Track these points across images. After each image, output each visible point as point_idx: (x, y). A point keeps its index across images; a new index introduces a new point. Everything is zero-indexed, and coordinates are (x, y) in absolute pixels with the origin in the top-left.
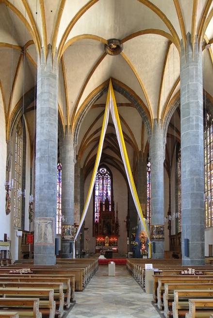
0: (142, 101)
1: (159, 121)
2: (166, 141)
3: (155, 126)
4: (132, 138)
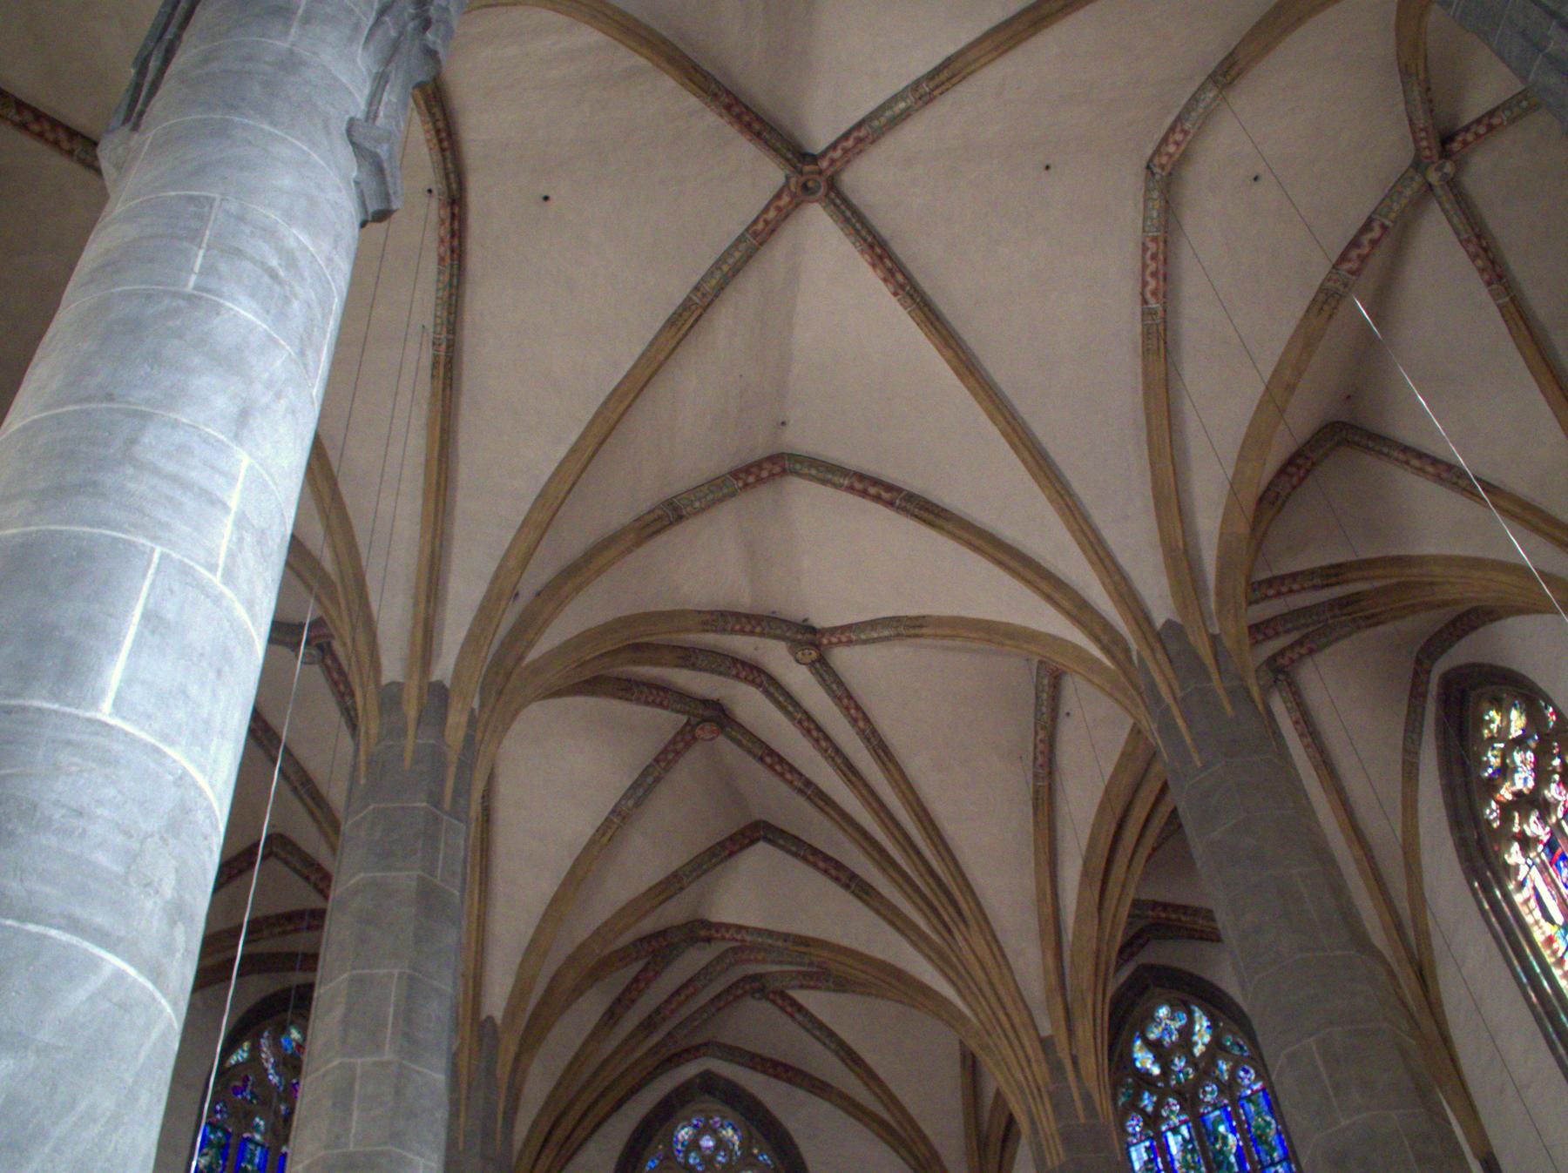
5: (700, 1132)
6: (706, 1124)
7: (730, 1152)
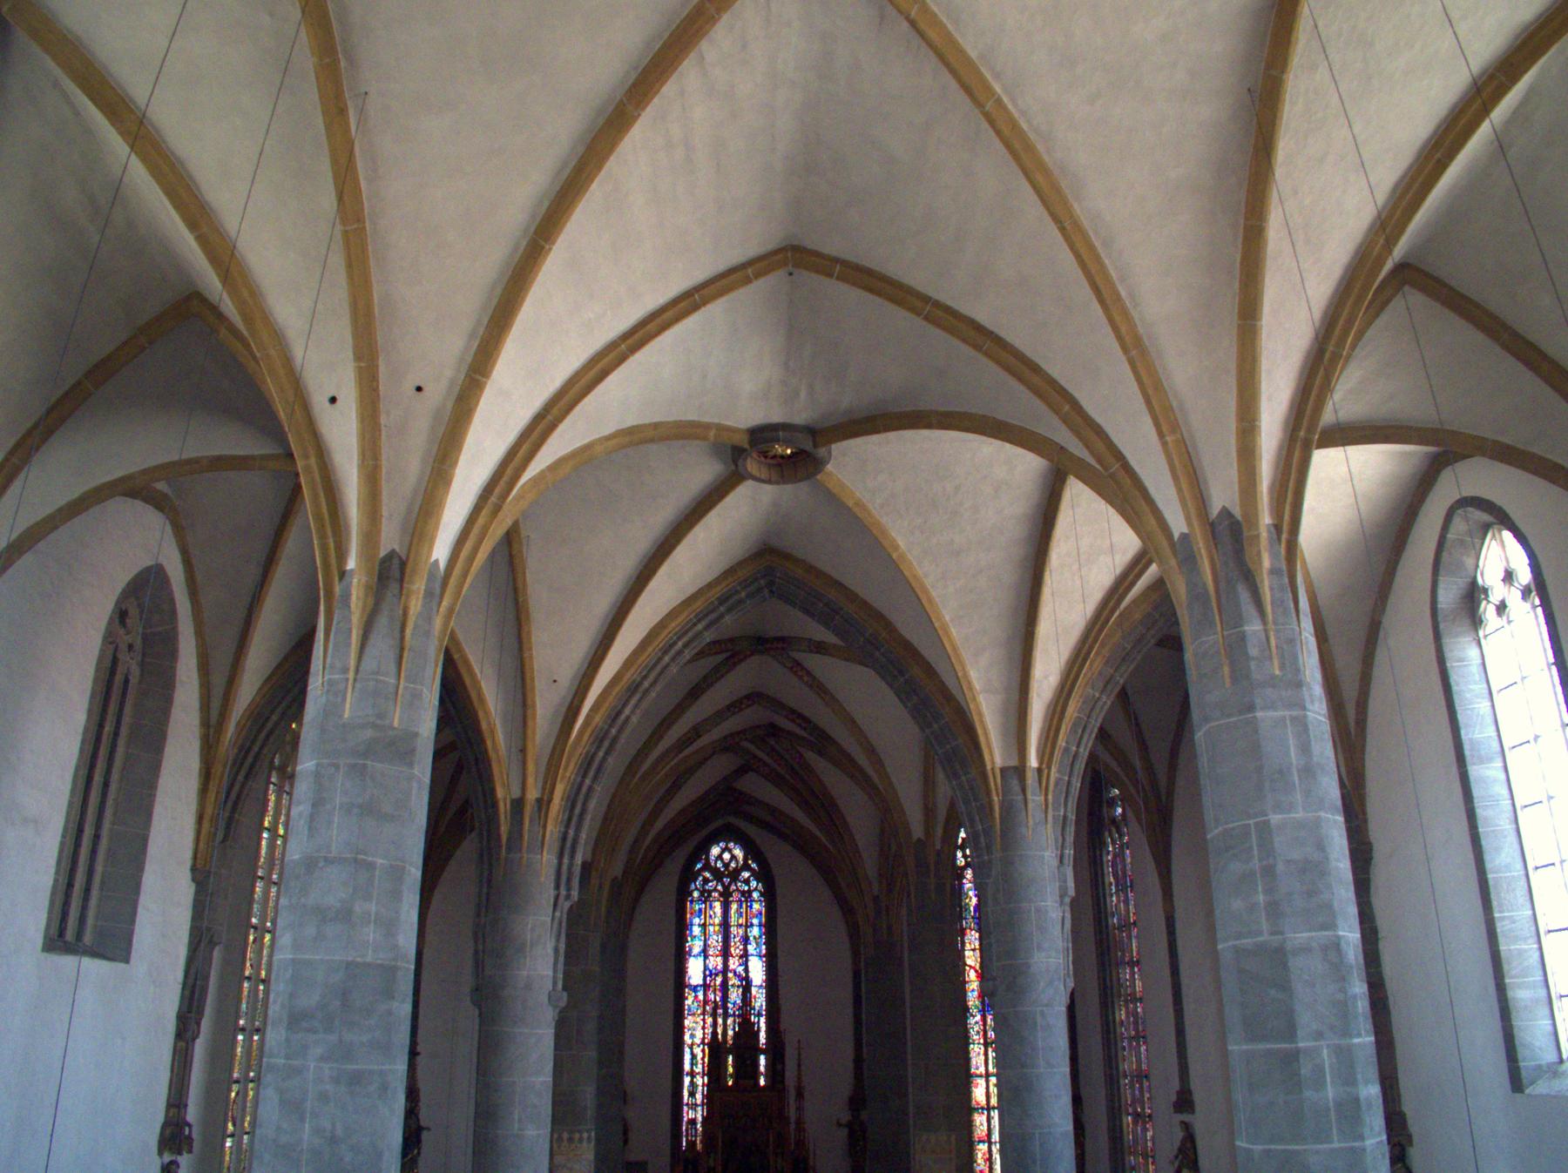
0: (930, 671)
2: (1071, 884)
3: (1008, 808)
7: (737, 861)
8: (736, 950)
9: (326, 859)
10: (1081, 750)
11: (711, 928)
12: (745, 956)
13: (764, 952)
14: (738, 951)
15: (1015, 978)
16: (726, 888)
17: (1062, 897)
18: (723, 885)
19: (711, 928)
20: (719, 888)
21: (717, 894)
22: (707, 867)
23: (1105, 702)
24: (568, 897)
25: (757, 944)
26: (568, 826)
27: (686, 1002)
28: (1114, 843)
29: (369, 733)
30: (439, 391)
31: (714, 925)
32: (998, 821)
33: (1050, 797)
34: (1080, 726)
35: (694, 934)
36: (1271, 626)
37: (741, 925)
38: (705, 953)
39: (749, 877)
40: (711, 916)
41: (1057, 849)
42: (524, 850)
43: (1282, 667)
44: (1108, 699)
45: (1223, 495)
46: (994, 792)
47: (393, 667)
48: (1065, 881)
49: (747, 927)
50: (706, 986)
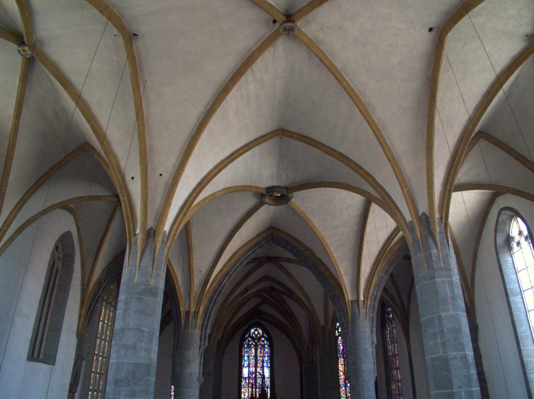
0: (327, 268)
1: (361, 304)
2: (375, 340)
3: (353, 314)
4: (307, 304)
5: (255, 331)
6: (256, 329)
7: (260, 334)
8: (259, 365)
9: (128, 328)
10: (378, 294)
11: (251, 357)
12: (263, 367)
13: (269, 366)
14: (260, 365)
15: (357, 372)
16: (256, 343)
17: (372, 344)
18: (255, 343)
19: (251, 357)
20: (254, 343)
21: (253, 346)
22: (250, 336)
23: (386, 278)
24: (204, 345)
25: (267, 363)
26: (204, 320)
27: (242, 383)
28: (389, 327)
29: (143, 287)
30: (167, 176)
31: (252, 356)
32: (350, 318)
33: (368, 310)
34: (378, 286)
35: (245, 359)
36: (440, 250)
37: (261, 356)
38: (249, 366)
39: (264, 340)
40: (251, 353)
41: (370, 328)
42: (190, 328)
43: (444, 264)
44: (387, 276)
45: (423, 208)
46: (348, 309)
47: (151, 265)
48: (373, 339)
49: (263, 357)
50: (249, 378)
